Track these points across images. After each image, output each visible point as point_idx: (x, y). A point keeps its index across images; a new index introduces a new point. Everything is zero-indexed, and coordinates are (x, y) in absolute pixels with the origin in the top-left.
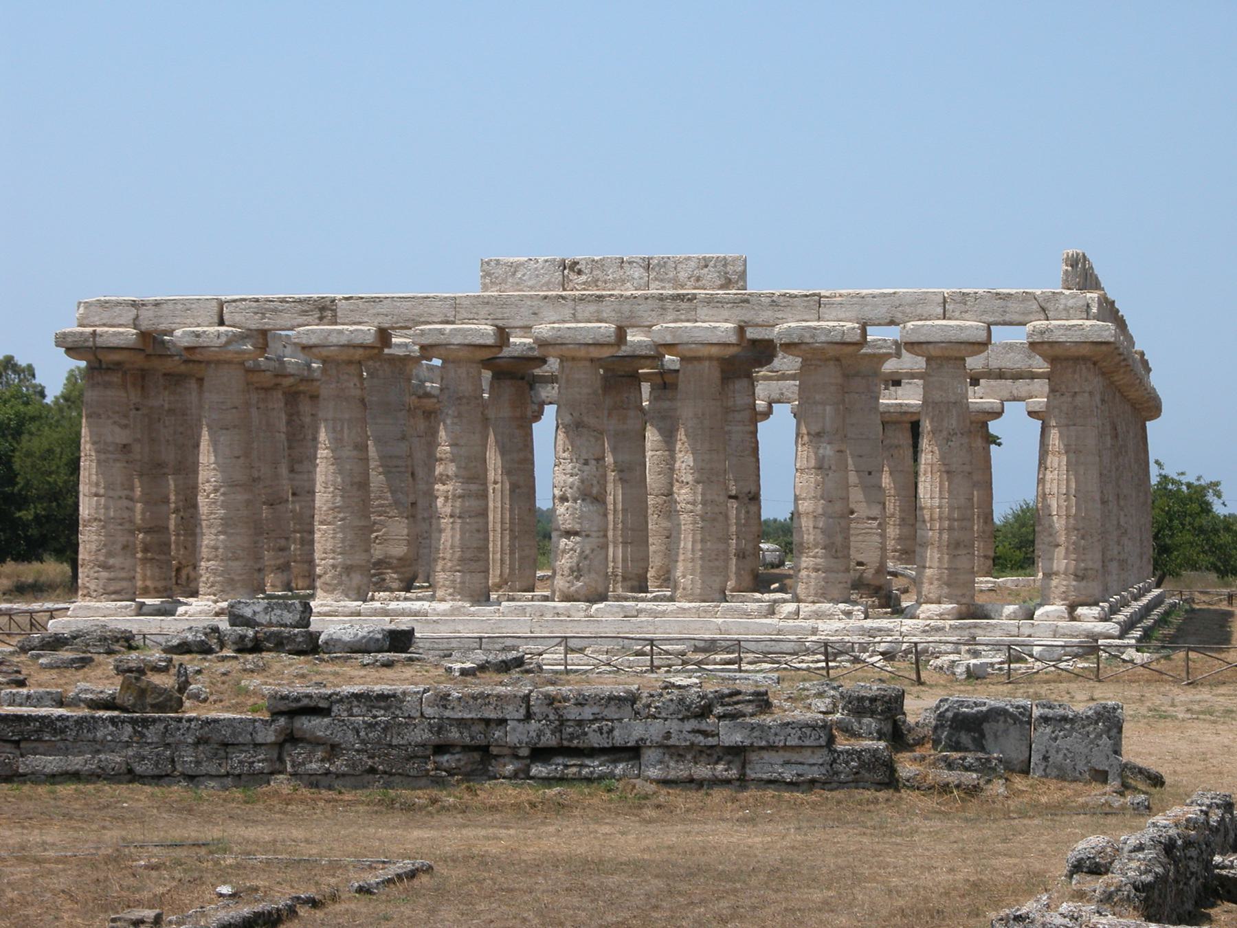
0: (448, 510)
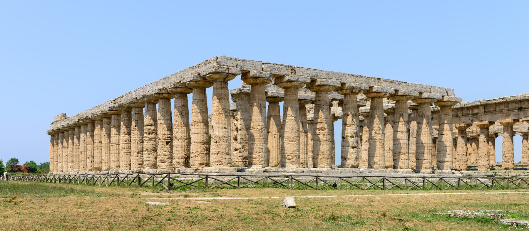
0: (325, 139)
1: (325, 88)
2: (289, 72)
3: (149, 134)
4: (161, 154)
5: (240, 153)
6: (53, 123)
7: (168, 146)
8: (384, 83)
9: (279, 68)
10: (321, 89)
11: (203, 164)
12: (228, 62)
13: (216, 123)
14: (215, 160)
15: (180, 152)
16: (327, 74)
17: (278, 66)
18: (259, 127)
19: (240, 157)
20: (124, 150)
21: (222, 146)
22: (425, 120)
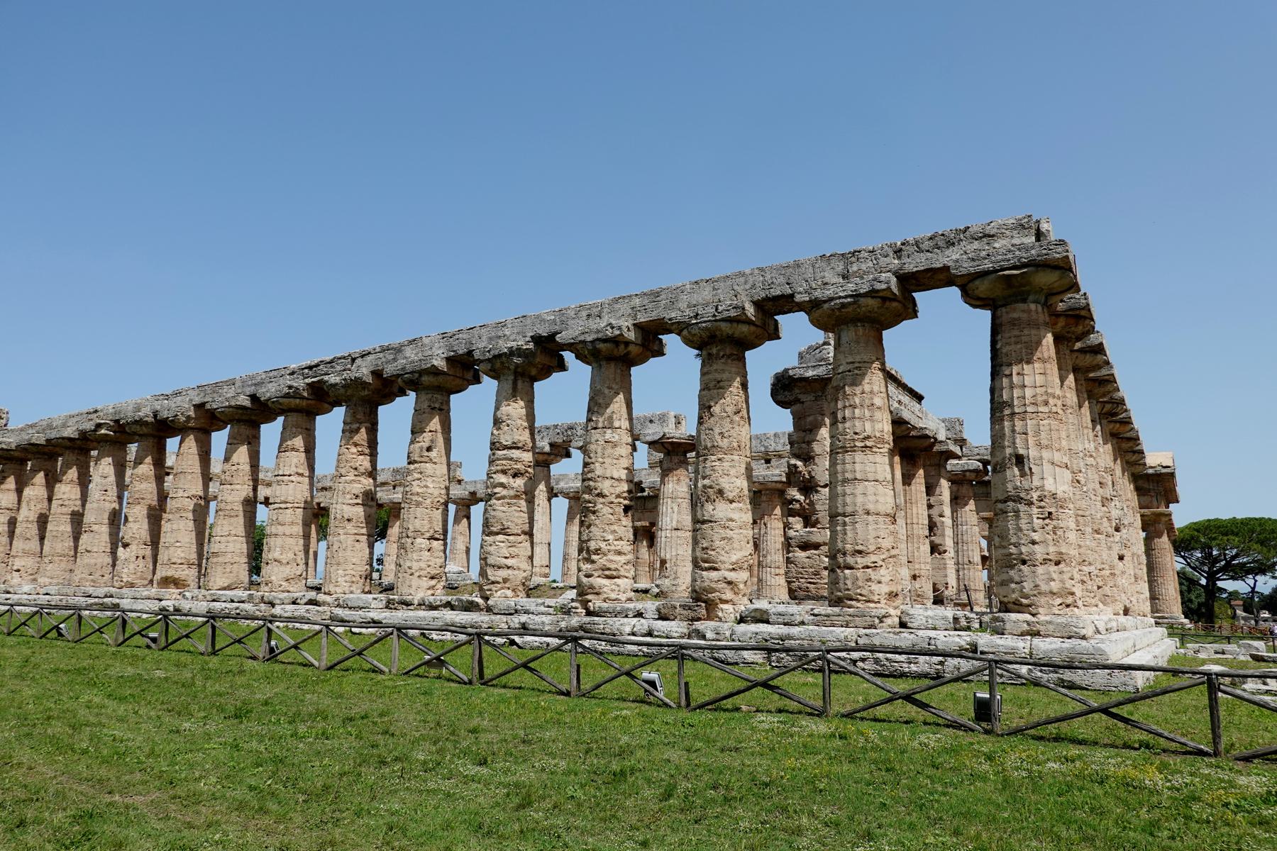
4: (603, 545)
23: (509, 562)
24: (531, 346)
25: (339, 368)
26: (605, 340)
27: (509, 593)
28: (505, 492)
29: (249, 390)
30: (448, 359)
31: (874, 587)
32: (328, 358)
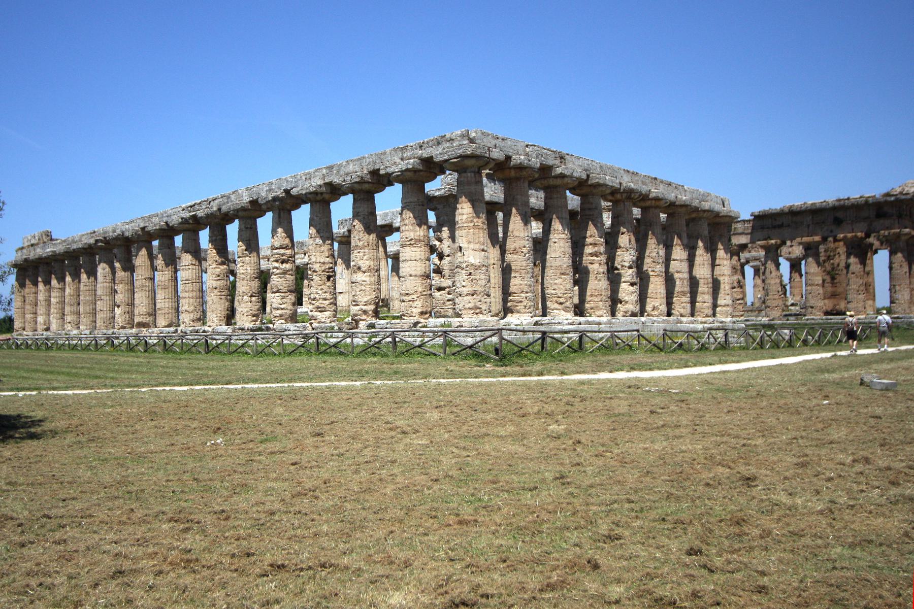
1: (601, 189)
2: (557, 162)
3: (282, 263)
4: (317, 296)
5: (449, 294)
6: (23, 248)
7: (329, 284)
8: (661, 186)
9: (546, 154)
10: (594, 191)
11: (426, 313)
12: (485, 140)
13: (469, 242)
14: (470, 305)
15: (368, 293)
16: (601, 167)
17: (545, 151)
18: (525, 250)
19: (449, 300)
20: (216, 292)
21: (480, 282)
22: (700, 244)
23: (282, 306)
24: (284, 195)
25: (204, 207)
26: (311, 193)
27: (283, 321)
28: (278, 271)
29: (165, 219)
30: (250, 202)
31: (414, 310)
32: (198, 201)
